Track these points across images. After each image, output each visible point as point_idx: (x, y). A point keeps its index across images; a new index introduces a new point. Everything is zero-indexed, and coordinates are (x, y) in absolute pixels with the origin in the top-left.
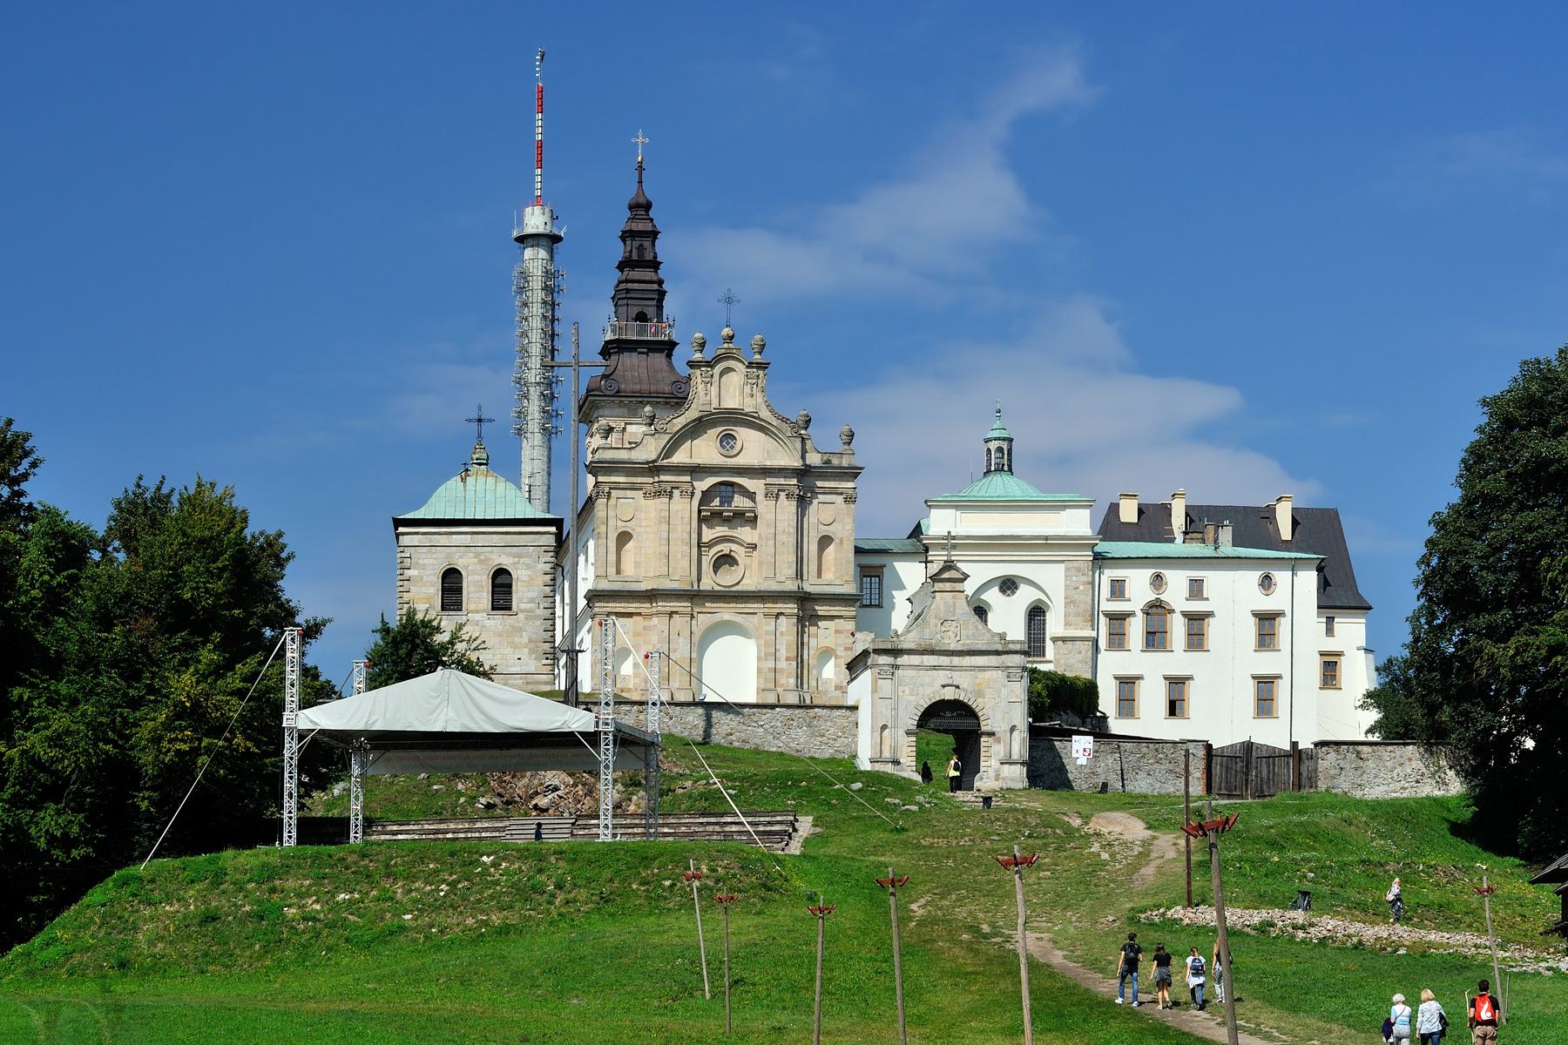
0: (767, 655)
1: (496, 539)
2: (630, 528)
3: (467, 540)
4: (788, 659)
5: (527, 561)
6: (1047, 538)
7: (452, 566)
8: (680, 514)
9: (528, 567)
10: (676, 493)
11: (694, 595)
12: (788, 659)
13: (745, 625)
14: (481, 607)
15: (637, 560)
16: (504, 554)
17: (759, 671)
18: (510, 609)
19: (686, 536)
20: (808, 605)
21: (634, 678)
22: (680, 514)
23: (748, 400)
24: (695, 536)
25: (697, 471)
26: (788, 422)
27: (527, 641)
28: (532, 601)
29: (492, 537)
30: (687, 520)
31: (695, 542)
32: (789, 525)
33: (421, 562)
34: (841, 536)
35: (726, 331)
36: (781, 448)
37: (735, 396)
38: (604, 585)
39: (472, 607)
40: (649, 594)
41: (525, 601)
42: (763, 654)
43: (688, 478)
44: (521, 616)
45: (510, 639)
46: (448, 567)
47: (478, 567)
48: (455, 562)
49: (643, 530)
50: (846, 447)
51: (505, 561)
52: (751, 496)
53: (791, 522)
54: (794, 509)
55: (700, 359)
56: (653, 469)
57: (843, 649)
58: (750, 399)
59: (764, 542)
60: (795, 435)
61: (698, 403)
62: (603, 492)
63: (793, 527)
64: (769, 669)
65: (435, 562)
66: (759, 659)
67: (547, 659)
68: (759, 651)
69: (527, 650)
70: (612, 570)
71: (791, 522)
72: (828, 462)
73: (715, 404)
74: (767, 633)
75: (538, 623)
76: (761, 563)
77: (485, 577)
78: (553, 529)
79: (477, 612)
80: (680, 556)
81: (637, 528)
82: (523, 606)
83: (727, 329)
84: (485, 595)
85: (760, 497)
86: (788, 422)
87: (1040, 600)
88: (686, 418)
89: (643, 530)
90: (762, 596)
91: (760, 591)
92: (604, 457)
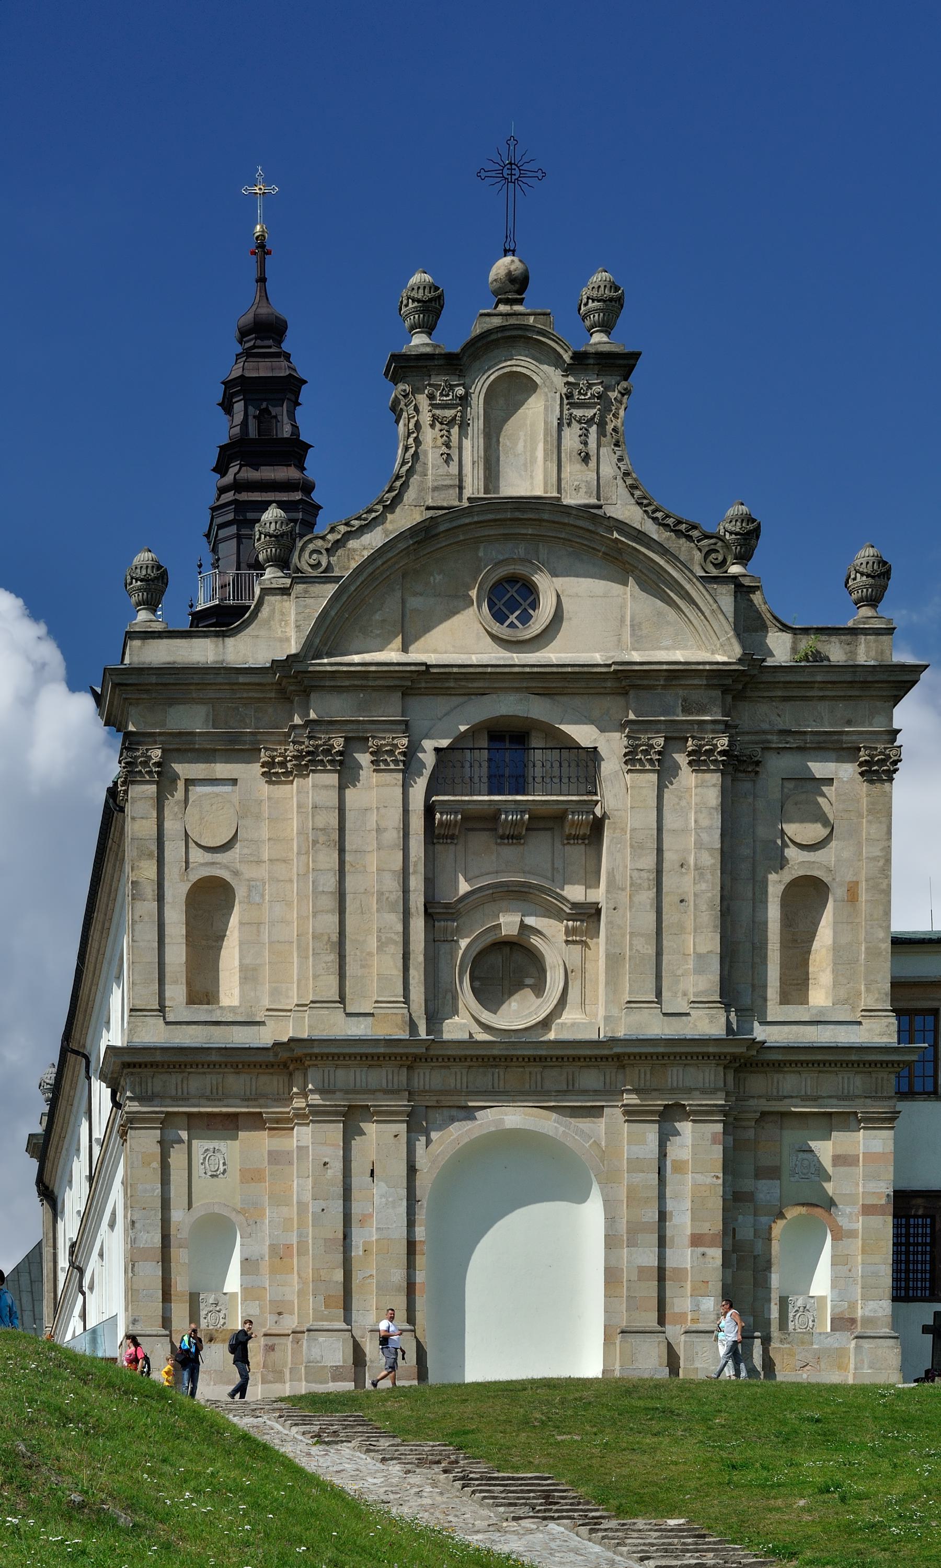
0: (634, 1229)
2: (226, 867)
4: (697, 1240)
8: (373, 818)
11: (417, 1058)
12: (697, 1240)
13: (569, 1143)
15: (247, 961)
17: (611, 1276)
19: (393, 886)
20: (757, 1083)
21: (244, 1300)
22: (373, 818)
23: (573, 471)
24: (417, 883)
26: (695, 533)
30: (393, 836)
31: (417, 901)
32: (699, 845)
34: (849, 877)
35: (504, 265)
36: (671, 614)
37: (533, 460)
40: (284, 1055)
42: (622, 1227)
49: (262, 872)
50: (865, 611)
53: (705, 837)
54: (713, 797)
55: (428, 350)
57: (858, 1208)
58: (579, 466)
59: (623, 898)
60: (714, 572)
61: (421, 490)
62: (145, 764)
63: (710, 850)
64: (641, 1270)
66: (611, 1242)
68: (610, 1220)
70: (176, 993)
71: (705, 837)
72: (818, 656)
73: (473, 487)
74: (635, 1165)
76: (614, 961)
80: (373, 944)
81: (243, 868)
83: (508, 259)
86: (695, 533)
88: (386, 533)
89: (262, 872)
90: (618, 1057)
91: (613, 1041)
92: (142, 659)
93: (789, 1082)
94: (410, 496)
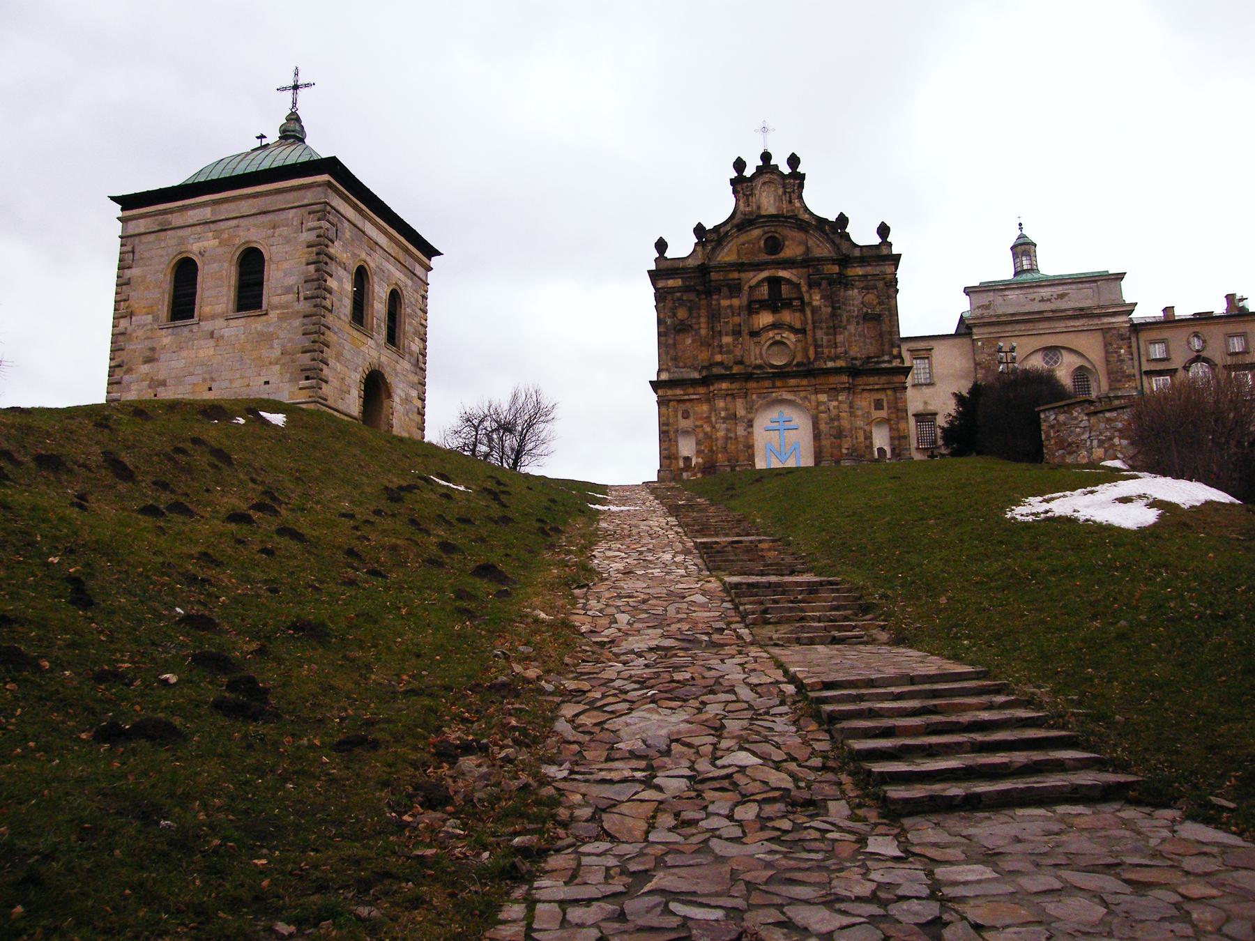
1: (246, 207)
3: (206, 213)
5: (284, 231)
6: (1082, 309)
7: (184, 255)
9: (288, 240)
10: (725, 290)
14: (219, 308)
16: (255, 225)
18: (259, 306)
25: (741, 267)
27: (279, 352)
28: (288, 290)
29: (243, 202)
33: (146, 255)
38: (664, 376)
39: (207, 310)
41: (279, 292)
43: (735, 275)
44: (273, 315)
45: (255, 354)
46: (180, 257)
47: (220, 251)
48: (189, 248)
51: (253, 234)
52: (798, 286)
56: (703, 270)
65: (163, 253)
67: (307, 378)
69: (278, 367)
75: (297, 323)
77: (226, 265)
78: (326, 177)
79: (213, 317)
82: (275, 300)
84: (225, 290)
85: (804, 289)
87: (1081, 368)
93: (872, 380)
94: (738, 215)
